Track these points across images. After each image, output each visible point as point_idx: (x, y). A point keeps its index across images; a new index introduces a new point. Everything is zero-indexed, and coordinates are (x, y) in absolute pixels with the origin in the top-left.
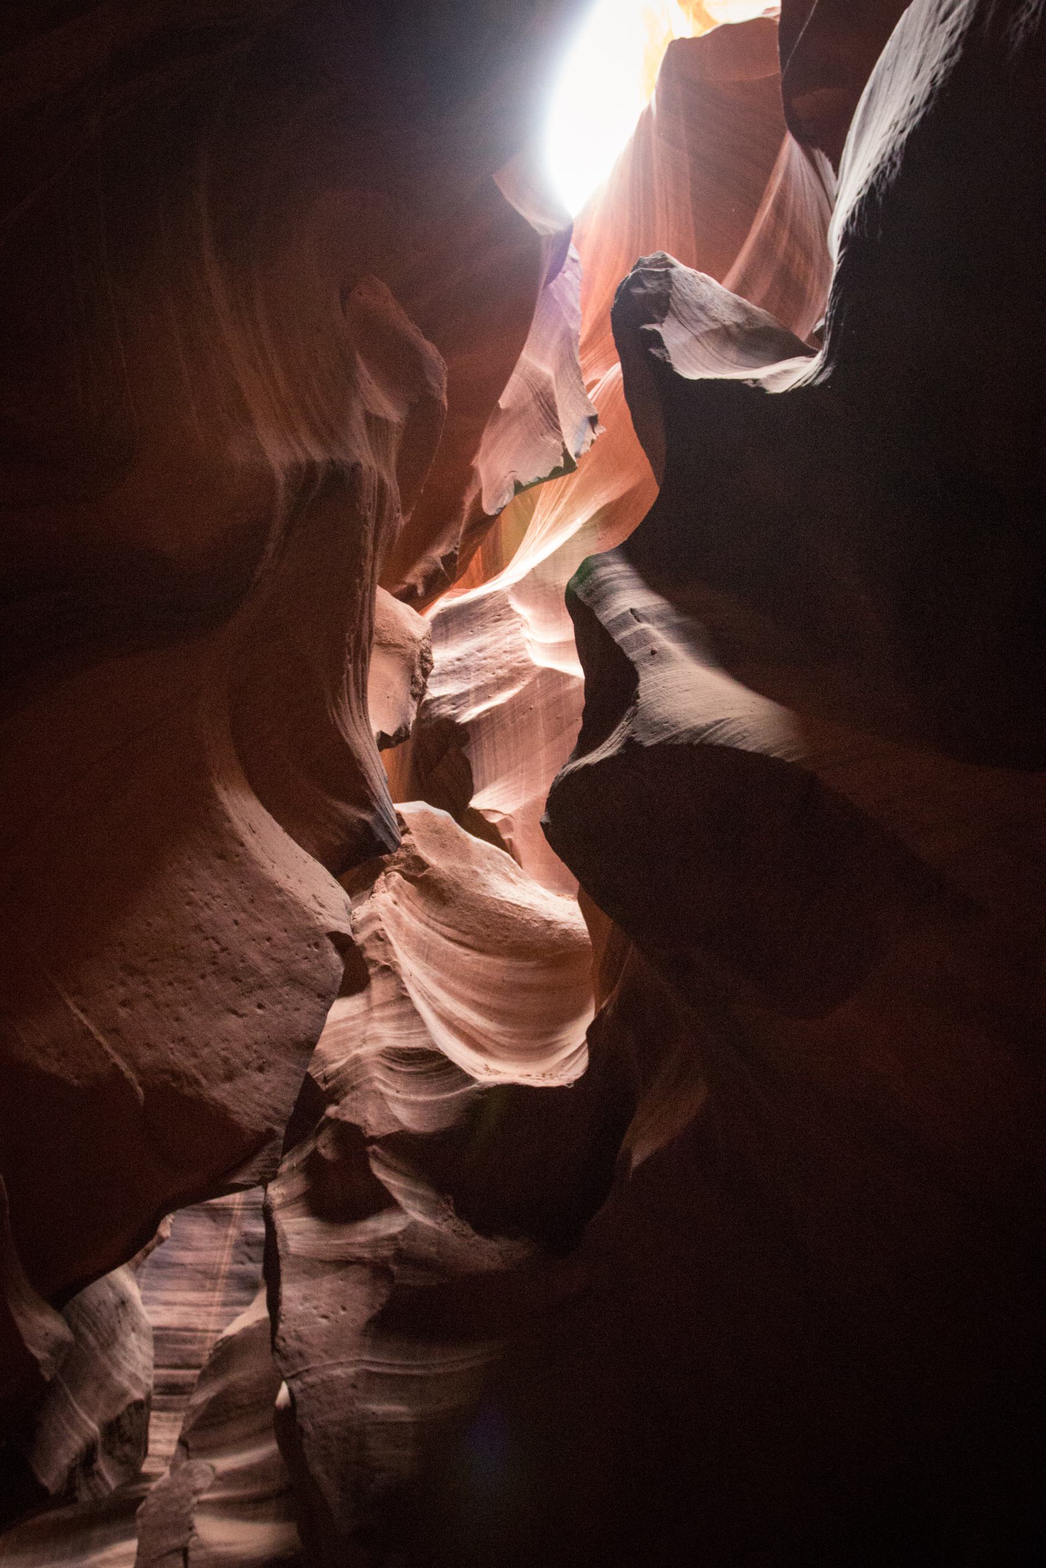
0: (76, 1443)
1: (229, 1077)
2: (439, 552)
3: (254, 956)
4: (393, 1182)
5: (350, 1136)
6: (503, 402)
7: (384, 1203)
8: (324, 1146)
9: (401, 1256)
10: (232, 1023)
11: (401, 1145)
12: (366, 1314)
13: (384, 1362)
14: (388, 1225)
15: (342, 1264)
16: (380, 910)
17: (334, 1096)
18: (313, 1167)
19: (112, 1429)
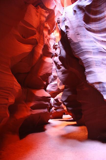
0: (50, 81)
1: (49, 71)
2: (55, 27)
3: (48, 66)
4: (61, 67)
5: (58, 65)
6: (55, 15)
7: (61, 68)
8: (57, 65)
9: (62, 70)
10: (48, 69)
11: (61, 65)
12: (61, 73)
13: (63, 75)
14: (61, 69)
15: (60, 71)
16: (57, 51)
17: (57, 63)
18: (57, 67)
19: (52, 80)
